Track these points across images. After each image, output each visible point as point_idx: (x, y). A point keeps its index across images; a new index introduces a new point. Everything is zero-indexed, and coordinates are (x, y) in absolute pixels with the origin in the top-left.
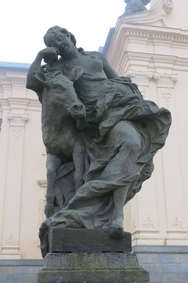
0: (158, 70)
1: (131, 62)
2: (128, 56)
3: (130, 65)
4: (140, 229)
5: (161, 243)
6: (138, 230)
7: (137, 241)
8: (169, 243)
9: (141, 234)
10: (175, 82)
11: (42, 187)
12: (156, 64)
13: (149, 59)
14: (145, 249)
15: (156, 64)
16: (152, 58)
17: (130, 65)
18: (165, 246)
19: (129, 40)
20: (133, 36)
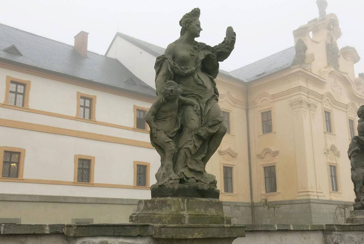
0: (310, 99)
1: (302, 93)
2: (300, 88)
3: (300, 94)
4: (310, 190)
5: (316, 198)
6: (308, 190)
7: (310, 197)
8: (320, 198)
9: (310, 193)
10: (316, 107)
11: (220, 154)
12: (310, 96)
13: (307, 92)
14: (313, 201)
15: (310, 96)
16: (309, 92)
17: (300, 94)
18: (318, 200)
19: (299, 77)
20: (302, 76)
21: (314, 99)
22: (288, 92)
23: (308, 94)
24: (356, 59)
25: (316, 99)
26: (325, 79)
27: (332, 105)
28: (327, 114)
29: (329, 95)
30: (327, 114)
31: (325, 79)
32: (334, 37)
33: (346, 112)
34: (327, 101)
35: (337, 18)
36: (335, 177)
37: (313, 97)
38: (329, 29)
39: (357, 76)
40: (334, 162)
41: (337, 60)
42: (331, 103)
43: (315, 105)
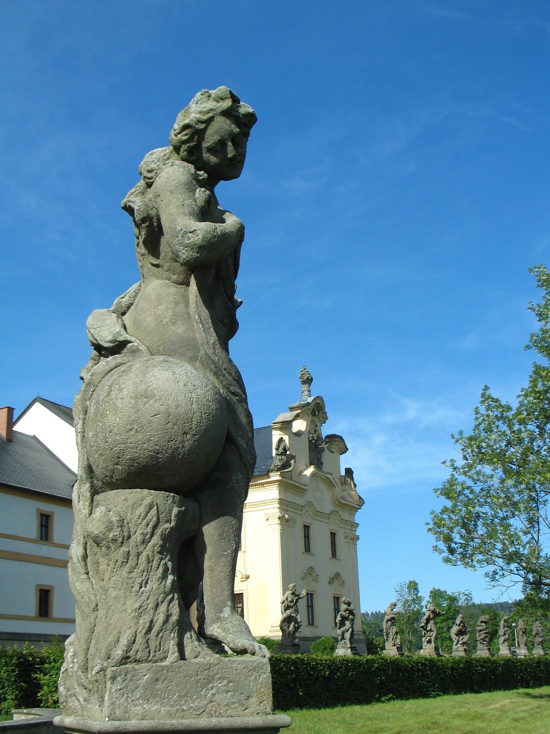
12: (289, 509)
15: (289, 509)
21: (293, 512)
22: (264, 503)
23: (287, 506)
24: (345, 450)
25: (295, 511)
26: (306, 485)
27: (313, 516)
28: (307, 528)
29: (310, 504)
30: (307, 528)
31: (306, 485)
32: (318, 424)
33: (328, 523)
34: (307, 512)
35: (323, 402)
36: (312, 607)
37: (292, 510)
38: (313, 414)
39: (343, 473)
40: (312, 589)
41: (321, 456)
42: (312, 515)
43: (293, 520)
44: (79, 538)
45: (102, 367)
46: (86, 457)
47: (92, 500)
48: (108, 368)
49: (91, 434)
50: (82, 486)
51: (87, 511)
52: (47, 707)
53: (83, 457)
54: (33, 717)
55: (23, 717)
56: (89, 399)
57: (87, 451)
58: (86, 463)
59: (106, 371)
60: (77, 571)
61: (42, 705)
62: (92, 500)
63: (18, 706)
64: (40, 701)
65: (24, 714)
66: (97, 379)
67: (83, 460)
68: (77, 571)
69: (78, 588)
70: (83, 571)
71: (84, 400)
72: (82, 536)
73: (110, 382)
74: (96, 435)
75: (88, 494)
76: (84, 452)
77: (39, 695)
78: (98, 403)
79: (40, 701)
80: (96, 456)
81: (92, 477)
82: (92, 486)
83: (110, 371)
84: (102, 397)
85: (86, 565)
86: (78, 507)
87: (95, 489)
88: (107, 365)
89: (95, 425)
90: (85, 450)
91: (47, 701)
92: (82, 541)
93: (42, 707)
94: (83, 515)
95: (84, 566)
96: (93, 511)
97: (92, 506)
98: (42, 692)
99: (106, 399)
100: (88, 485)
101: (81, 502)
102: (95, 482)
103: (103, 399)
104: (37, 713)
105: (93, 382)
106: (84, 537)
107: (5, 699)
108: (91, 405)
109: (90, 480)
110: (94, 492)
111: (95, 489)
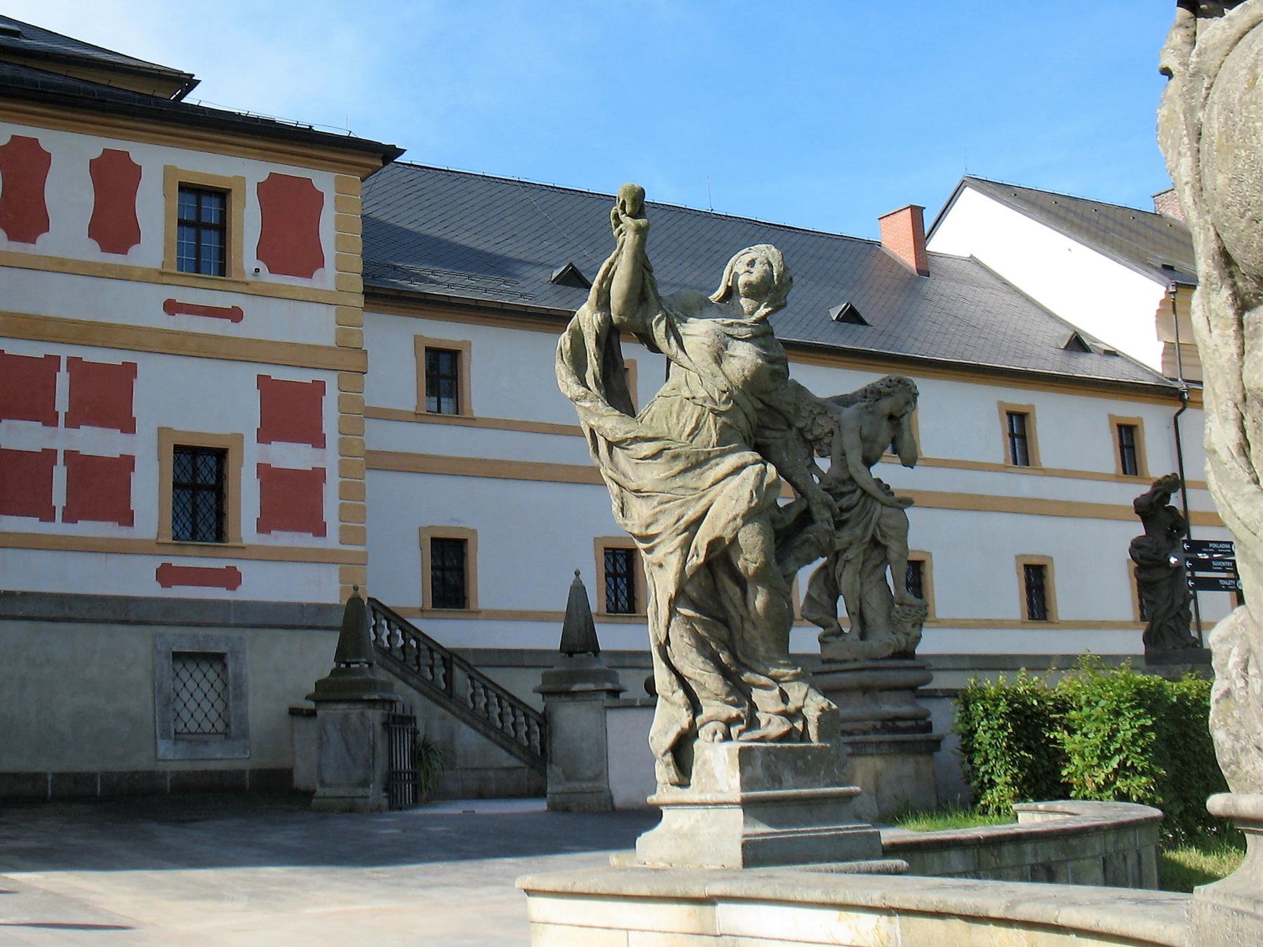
44: (1223, 407)
45: (1219, 33)
46: (1212, 233)
47: (1241, 325)
48: (1233, 32)
49: (1221, 179)
50: (1213, 296)
51: (1233, 349)
52: (1085, 798)
53: (1206, 235)
54: (1059, 817)
55: (1038, 818)
56: (1203, 106)
57: (1216, 216)
58: (1214, 245)
59: (1232, 39)
60: (1233, 477)
61: (1073, 794)
62: (1241, 325)
63: (1021, 798)
64: (1069, 786)
65: (1039, 811)
66: (1212, 60)
67: (1206, 240)
68: (1233, 477)
69: (1240, 515)
70: (1247, 477)
71: (1190, 111)
72: (1230, 404)
73: (1250, 61)
74: (1237, 179)
75: (1230, 313)
76: (1206, 222)
77: (1064, 773)
78: (1228, 109)
79: (1069, 786)
80: (1243, 224)
81: (1231, 275)
82: (1236, 294)
83: (1240, 38)
84: (1237, 96)
85: (1250, 463)
86: (1210, 343)
87: (1242, 300)
88: (1231, 27)
89: (1230, 158)
90: (1209, 218)
91: (1083, 785)
92: (1232, 414)
93: (1075, 798)
94: (1226, 357)
95: (1245, 467)
96: (1247, 348)
97: (1243, 336)
98: (1071, 769)
99: (1247, 98)
100: (1226, 293)
101: (1216, 332)
102: (1240, 284)
103: (1241, 98)
104: (1067, 809)
105: (1205, 67)
106: (1236, 405)
107: (992, 784)
108: (1209, 119)
109: (1229, 281)
110: (1243, 306)
111: (1242, 300)
